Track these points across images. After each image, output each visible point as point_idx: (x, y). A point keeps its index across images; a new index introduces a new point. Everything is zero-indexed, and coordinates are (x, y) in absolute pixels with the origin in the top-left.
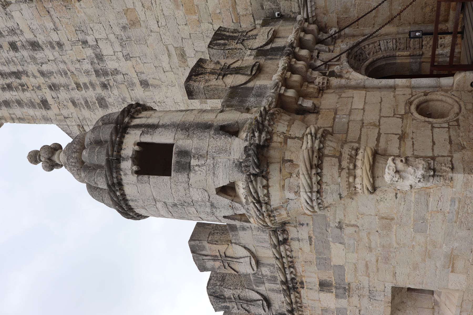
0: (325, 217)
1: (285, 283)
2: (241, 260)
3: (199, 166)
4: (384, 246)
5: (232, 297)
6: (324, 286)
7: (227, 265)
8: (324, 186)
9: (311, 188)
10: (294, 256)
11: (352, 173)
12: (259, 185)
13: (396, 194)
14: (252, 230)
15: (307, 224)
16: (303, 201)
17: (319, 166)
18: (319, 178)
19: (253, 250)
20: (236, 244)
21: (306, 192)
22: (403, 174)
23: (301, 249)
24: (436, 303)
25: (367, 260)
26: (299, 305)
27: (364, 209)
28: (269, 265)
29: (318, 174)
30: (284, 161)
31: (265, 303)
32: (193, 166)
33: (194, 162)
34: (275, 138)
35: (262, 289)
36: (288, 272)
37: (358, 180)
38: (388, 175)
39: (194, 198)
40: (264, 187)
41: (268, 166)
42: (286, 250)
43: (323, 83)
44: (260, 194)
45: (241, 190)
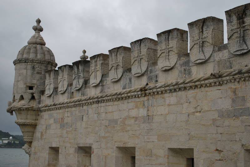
5: (246, 24)
26: (247, 79)
31: (245, 51)
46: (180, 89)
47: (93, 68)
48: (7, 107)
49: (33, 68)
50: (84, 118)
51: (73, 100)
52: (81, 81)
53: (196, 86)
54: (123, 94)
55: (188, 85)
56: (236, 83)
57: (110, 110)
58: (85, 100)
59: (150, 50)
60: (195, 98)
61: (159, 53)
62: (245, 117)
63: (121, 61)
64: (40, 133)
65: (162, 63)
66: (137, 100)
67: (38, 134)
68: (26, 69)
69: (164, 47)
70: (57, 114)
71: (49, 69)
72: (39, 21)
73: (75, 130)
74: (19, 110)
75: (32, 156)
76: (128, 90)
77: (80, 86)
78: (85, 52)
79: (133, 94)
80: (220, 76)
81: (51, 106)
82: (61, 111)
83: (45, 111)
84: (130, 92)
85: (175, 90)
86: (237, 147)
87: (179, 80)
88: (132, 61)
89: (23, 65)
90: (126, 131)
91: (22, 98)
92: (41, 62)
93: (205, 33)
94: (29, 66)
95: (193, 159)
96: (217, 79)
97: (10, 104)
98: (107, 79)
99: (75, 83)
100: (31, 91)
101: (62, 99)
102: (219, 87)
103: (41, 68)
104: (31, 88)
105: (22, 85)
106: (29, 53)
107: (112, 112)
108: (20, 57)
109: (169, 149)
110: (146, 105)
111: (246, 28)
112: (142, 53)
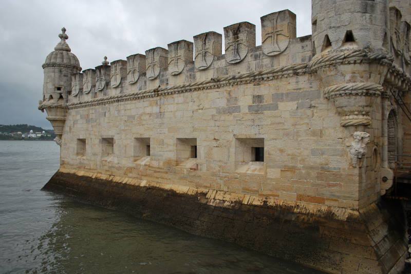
0: (319, 97)
1: (260, 74)
2: (276, 45)
3: (366, 19)
4: (298, 132)
6: (258, 98)
7: (270, 35)
8: (354, 97)
9: (355, 90)
10: (282, 79)
11: (360, 113)
12: (356, 58)
13: (341, 138)
14: (302, 52)
15: (311, 87)
16: (345, 85)
17: (367, 94)
18: (360, 94)
19: (285, 53)
20: (290, 41)
21: (352, 87)
22: (361, 142)
23: (289, 83)
24: (247, 163)
25: (285, 124)
26: (239, 83)
27: (326, 120)
28: (273, 63)
29: (362, 93)
30: (370, 73)
31: (239, 61)
32: (365, 15)
33: (368, 15)
34: (382, 67)
35: (249, 59)
36: (269, 75)
37: (355, 117)
38: (359, 134)
39: (342, 15)
40: (355, 61)
41: (368, 63)
42: (288, 74)
43: (386, 95)
44: (350, 59)
45: (351, 47)
46: (186, 91)
47: (113, 72)
48: (38, 106)
49: (61, 71)
50: (107, 114)
51: (96, 99)
52: (103, 83)
53: (199, 88)
54: (140, 94)
55: (193, 87)
56: (231, 86)
57: (129, 108)
58: (107, 99)
59: (162, 58)
60: (198, 98)
61: (169, 60)
62: (236, 113)
63: (137, 66)
64: (68, 128)
65: (172, 69)
66: (151, 99)
67: (67, 128)
68: (54, 72)
69: (173, 56)
70: (82, 111)
71: (75, 72)
72: (64, 30)
73: (99, 125)
74: (50, 108)
75: (62, 146)
76: (143, 91)
77: (102, 88)
78: (106, 58)
79: (147, 94)
80: (219, 81)
81: (77, 104)
82: (86, 109)
83: (72, 108)
84: (145, 93)
85: (182, 91)
86: (230, 137)
87: (185, 84)
88: (147, 67)
89: (51, 69)
90: (143, 125)
91: (51, 97)
92: (67, 66)
93: (207, 44)
94: (57, 70)
95: (196, 147)
96: (216, 83)
97: (41, 103)
98: (126, 81)
99: (97, 84)
100: (59, 91)
101: (87, 98)
102: (217, 90)
103: (67, 71)
104: (59, 89)
105: (50, 86)
106: (56, 58)
107: (130, 109)
108: (48, 62)
109: (177, 139)
110: (159, 103)
111: (239, 42)
112: (156, 60)
